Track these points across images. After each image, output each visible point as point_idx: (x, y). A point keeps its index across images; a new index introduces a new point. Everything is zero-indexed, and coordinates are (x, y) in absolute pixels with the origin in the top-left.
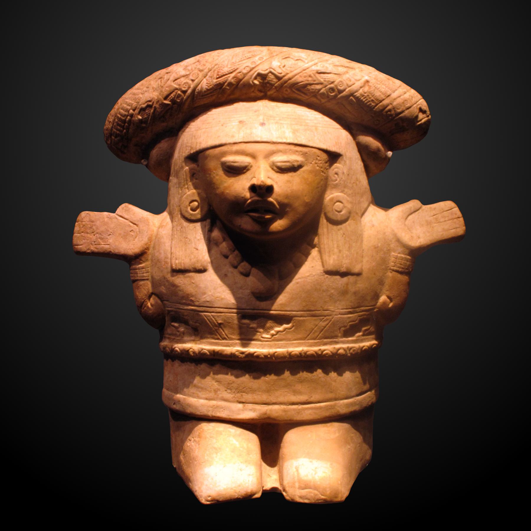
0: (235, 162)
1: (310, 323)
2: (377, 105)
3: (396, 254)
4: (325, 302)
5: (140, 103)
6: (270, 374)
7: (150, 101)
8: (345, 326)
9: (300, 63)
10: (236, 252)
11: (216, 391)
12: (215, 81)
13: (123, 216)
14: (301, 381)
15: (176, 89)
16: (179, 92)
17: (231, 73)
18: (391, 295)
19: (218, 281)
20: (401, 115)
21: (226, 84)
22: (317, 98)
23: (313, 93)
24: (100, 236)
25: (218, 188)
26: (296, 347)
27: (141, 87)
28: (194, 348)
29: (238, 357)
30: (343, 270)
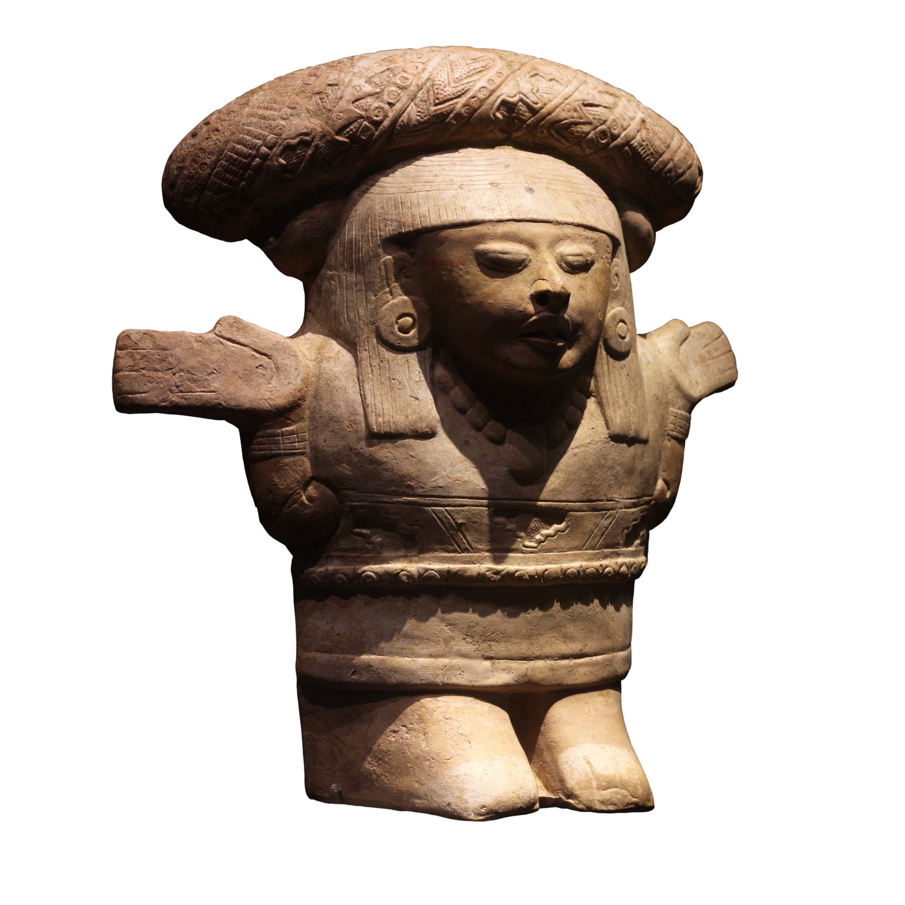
0: (505, 253)
1: (591, 521)
2: (656, 160)
3: (676, 410)
4: (610, 486)
5: (284, 136)
6: (533, 609)
7: (306, 134)
8: (628, 528)
9: (558, 87)
10: (478, 404)
11: (447, 641)
12: (433, 108)
13: (234, 338)
14: (574, 619)
15: (361, 117)
16: (366, 123)
17: (459, 96)
18: (669, 478)
19: (457, 453)
20: (682, 179)
21: (451, 115)
22: (581, 147)
23: (577, 137)
24: (189, 375)
25: (470, 295)
26: (571, 561)
27: (275, 106)
28: (408, 569)
29: (489, 579)
30: (632, 433)
